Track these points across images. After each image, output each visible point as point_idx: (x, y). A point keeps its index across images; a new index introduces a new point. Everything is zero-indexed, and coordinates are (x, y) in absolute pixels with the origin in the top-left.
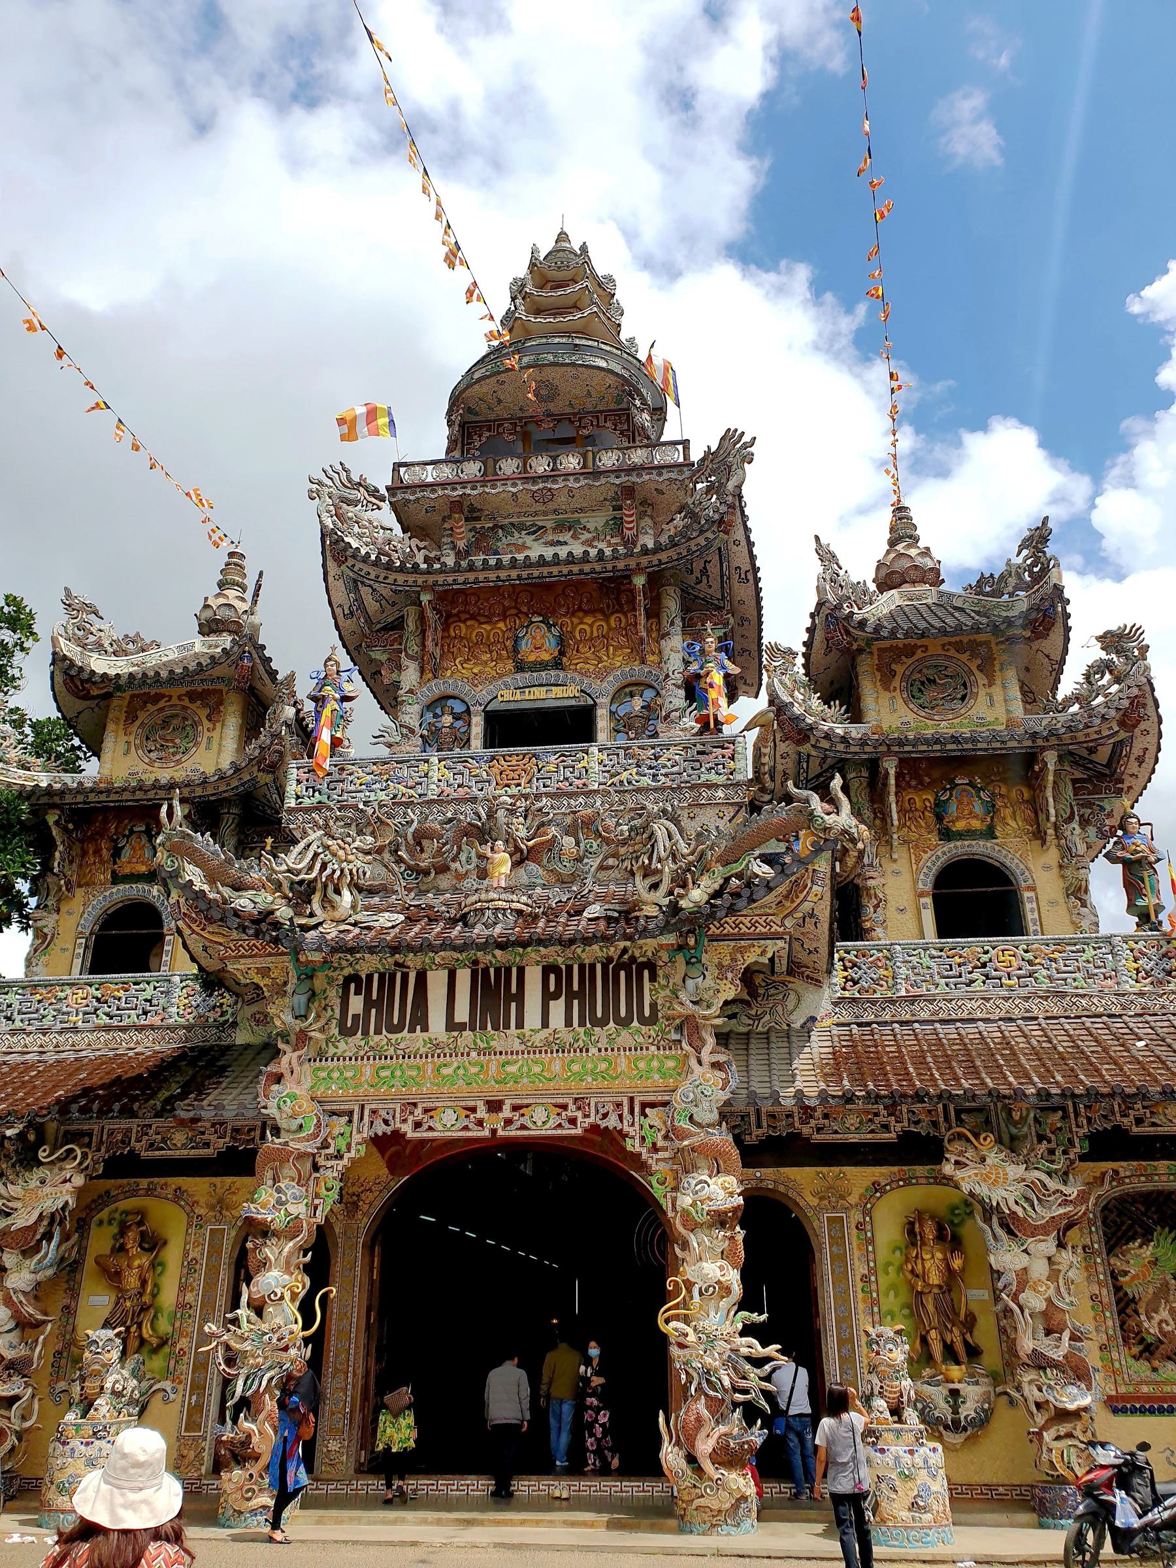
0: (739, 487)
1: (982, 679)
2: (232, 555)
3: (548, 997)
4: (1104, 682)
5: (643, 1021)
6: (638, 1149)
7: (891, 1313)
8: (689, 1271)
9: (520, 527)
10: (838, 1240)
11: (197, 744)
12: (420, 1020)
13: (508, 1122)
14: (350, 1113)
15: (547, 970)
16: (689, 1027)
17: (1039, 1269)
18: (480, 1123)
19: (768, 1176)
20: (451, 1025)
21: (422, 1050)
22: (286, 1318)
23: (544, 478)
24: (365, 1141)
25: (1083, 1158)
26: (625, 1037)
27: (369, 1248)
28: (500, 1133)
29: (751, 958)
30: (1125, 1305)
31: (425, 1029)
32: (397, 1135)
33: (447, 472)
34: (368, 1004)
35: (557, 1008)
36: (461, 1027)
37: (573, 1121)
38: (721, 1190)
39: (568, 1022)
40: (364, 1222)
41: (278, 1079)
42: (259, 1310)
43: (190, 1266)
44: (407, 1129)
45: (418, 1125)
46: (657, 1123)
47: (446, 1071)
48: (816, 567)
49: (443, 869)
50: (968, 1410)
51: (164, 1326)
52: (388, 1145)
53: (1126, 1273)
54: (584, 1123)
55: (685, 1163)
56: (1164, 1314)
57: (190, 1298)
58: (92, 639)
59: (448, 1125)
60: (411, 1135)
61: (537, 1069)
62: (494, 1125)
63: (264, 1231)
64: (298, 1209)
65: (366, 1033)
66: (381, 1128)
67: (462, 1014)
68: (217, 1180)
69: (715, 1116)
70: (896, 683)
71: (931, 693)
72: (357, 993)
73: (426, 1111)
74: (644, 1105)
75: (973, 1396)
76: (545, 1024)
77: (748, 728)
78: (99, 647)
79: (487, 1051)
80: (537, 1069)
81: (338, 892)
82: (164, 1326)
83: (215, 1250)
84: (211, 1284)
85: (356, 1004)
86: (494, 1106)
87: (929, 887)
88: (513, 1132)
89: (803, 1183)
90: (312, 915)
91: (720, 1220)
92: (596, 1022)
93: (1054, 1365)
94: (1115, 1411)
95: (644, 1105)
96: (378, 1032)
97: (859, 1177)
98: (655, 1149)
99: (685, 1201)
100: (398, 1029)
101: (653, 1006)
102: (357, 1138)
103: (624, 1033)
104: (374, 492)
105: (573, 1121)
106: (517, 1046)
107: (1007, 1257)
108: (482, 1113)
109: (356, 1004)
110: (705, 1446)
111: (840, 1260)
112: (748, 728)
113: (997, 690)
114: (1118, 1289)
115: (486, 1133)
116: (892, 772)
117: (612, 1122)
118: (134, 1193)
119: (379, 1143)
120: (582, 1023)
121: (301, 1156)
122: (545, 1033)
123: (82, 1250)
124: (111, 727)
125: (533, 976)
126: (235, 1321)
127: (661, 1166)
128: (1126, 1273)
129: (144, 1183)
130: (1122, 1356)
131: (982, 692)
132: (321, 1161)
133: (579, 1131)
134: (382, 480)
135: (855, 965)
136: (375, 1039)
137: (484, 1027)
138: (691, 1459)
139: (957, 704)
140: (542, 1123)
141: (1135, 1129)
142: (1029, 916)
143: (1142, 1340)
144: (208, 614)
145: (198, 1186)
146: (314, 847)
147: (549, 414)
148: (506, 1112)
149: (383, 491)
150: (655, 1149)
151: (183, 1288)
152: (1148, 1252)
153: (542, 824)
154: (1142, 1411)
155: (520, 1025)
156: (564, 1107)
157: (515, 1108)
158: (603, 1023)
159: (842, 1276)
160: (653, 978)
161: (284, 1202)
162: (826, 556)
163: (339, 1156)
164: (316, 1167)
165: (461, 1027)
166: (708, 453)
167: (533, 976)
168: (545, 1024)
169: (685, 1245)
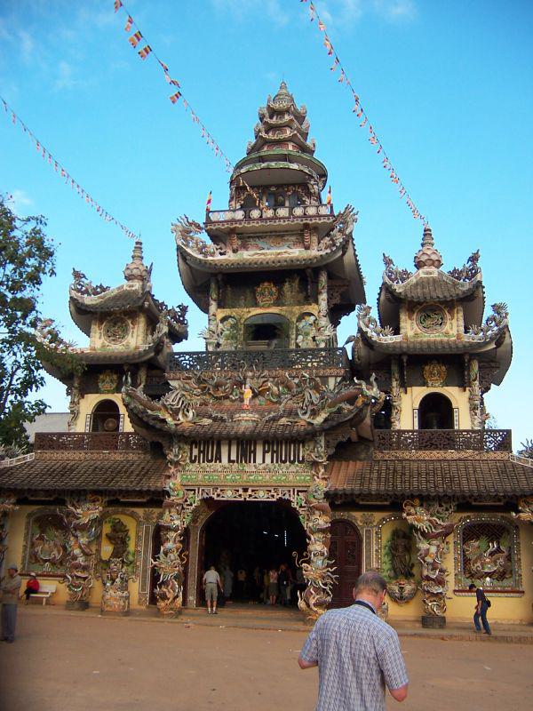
0: (351, 233)
1: (448, 316)
2: (137, 243)
4: (492, 325)
5: (299, 462)
6: (295, 506)
7: (385, 562)
8: (311, 547)
10: (368, 538)
11: (128, 334)
12: (219, 459)
13: (250, 496)
14: (194, 490)
16: (315, 464)
17: (433, 549)
18: (240, 496)
19: (343, 515)
20: (230, 461)
21: (219, 470)
22: (174, 556)
23: (270, 219)
24: (200, 500)
25: (454, 512)
26: (293, 468)
27: (202, 531)
28: (248, 499)
30: (466, 561)
31: (220, 462)
32: (211, 498)
33: (229, 216)
34: (200, 452)
35: (268, 457)
36: (233, 462)
37: (273, 496)
38: (322, 521)
39: (272, 462)
40: (200, 525)
41: (169, 477)
42: (166, 554)
43: (138, 537)
44: (215, 497)
45: (218, 495)
46: (303, 498)
47: (228, 477)
48: (383, 267)
49: (227, 397)
50: (406, 593)
51: (131, 558)
52: (208, 502)
53: (468, 551)
54: (277, 497)
55: (312, 510)
56: (479, 564)
57: (139, 549)
58: (84, 288)
59: (229, 495)
60: (216, 498)
61: (260, 478)
62: (245, 497)
63: (168, 529)
64: (177, 522)
65: (199, 462)
66: (205, 496)
67: (233, 457)
68: (147, 509)
69: (323, 496)
70: (414, 316)
71: (429, 322)
72: (196, 447)
73: (221, 490)
74: (298, 491)
75: (408, 588)
76: (264, 462)
77: (347, 342)
78: (86, 292)
80: (260, 478)
81: (188, 411)
82: (131, 558)
83: (147, 533)
84: (146, 546)
85: (195, 452)
86: (245, 490)
88: (251, 499)
89: (358, 517)
90: (179, 420)
91: (322, 531)
92: (282, 462)
93: (433, 580)
95: (298, 491)
96: (204, 462)
97: (378, 516)
98: (301, 507)
99: (310, 524)
100: (211, 461)
101: (303, 457)
102: (197, 499)
103: (292, 466)
104: (198, 227)
105: (273, 496)
106: (254, 470)
107: (423, 545)
108: (241, 492)
109: (195, 452)
110: (312, 601)
111: (369, 544)
112: (347, 342)
113: (454, 321)
114: (464, 556)
115: (242, 499)
116: (405, 360)
117: (287, 497)
118: (117, 513)
119: (204, 500)
120: (277, 462)
121: (179, 504)
122: (264, 465)
123: (101, 532)
124: (93, 327)
126: (159, 558)
127: (303, 513)
128: (468, 551)
129: (120, 509)
130: (462, 578)
131: (449, 322)
132: (185, 506)
133: (275, 500)
134: (201, 220)
135: (384, 438)
136: (203, 465)
137: (241, 462)
138: (308, 605)
139: (438, 327)
140: (262, 496)
141: (474, 503)
142: (455, 418)
143: (470, 573)
144: (129, 272)
145: (140, 511)
146: (179, 396)
148: (250, 492)
149: (202, 225)
150: (301, 507)
151: (136, 546)
152: (477, 544)
153: (264, 382)
155: (255, 462)
156: (270, 491)
157: (253, 491)
158: (285, 462)
159: (369, 551)
160: (303, 447)
161: (175, 520)
162: (388, 262)
163: (191, 505)
164: (183, 508)
165: (233, 462)
166: (340, 214)
168: (264, 462)
169: (310, 539)
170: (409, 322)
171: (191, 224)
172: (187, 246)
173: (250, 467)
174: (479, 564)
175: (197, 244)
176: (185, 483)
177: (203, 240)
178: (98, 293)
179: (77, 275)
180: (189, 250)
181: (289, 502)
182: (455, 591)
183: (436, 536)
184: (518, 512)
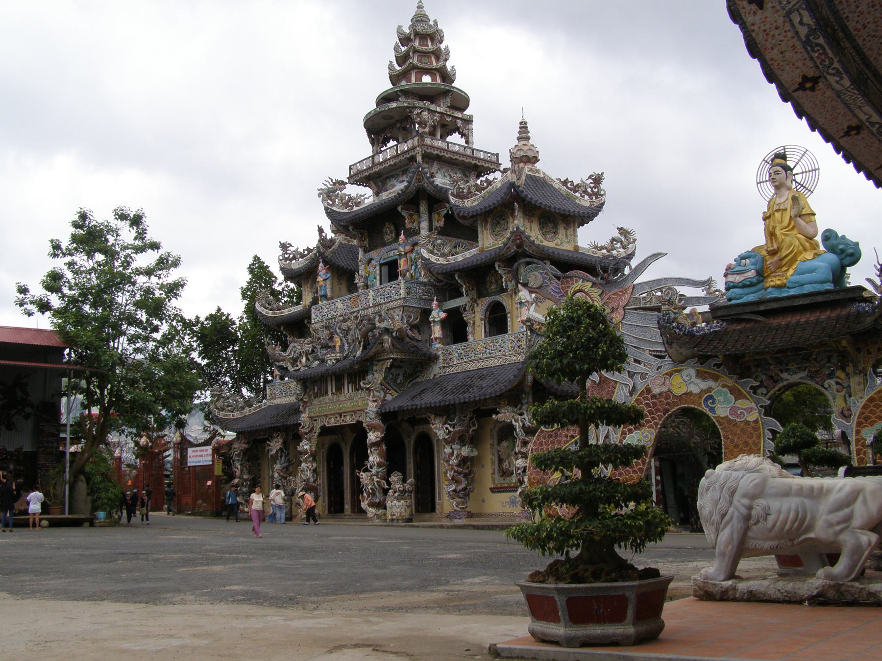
3: (348, 383)
9: (392, 176)
12: (327, 393)
15: (349, 375)
20: (333, 394)
29: (385, 367)
30: (501, 461)
35: (350, 386)
70: (488, 226)
78: (294, 258)
79: (338, 401)
87: (483, 317)
94: (493, 492)
104: (342, 183)
125: (346, 376)
130: (497, 476)
134: (344, 177)
147: (397, 121)
149: (347, 181)
154: (499, 492)
167: (346, 376)
170: (485, 232)
171: (334, 184)
172: (333, 204)
173: (342, 398)
174: (507, 463)
175: (342, 200)
176: (312, 415)
177: (348, 193)
178: (305, 256)
179: (284, 246)
180: (335, 208)
181: (362, 423)
182: (491, 489)
183: (453, 441)
184: (497, 413)
